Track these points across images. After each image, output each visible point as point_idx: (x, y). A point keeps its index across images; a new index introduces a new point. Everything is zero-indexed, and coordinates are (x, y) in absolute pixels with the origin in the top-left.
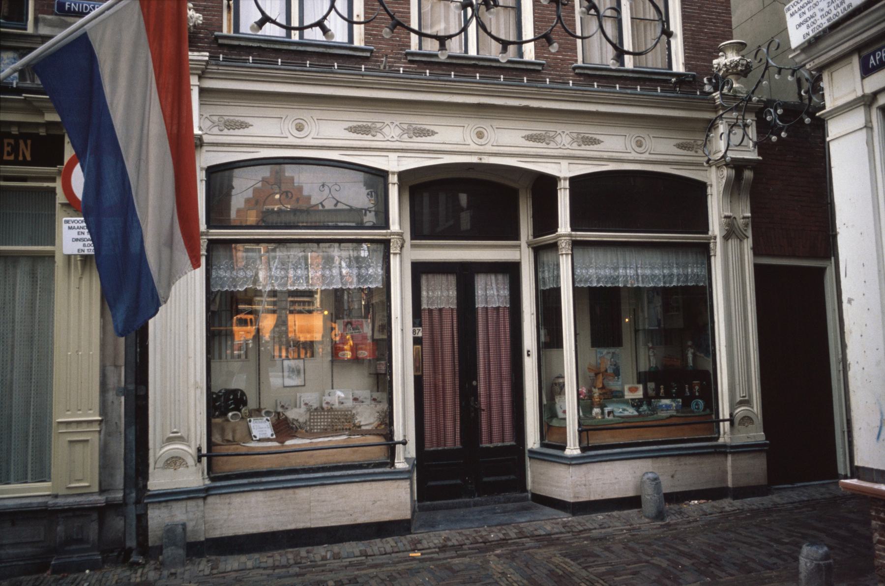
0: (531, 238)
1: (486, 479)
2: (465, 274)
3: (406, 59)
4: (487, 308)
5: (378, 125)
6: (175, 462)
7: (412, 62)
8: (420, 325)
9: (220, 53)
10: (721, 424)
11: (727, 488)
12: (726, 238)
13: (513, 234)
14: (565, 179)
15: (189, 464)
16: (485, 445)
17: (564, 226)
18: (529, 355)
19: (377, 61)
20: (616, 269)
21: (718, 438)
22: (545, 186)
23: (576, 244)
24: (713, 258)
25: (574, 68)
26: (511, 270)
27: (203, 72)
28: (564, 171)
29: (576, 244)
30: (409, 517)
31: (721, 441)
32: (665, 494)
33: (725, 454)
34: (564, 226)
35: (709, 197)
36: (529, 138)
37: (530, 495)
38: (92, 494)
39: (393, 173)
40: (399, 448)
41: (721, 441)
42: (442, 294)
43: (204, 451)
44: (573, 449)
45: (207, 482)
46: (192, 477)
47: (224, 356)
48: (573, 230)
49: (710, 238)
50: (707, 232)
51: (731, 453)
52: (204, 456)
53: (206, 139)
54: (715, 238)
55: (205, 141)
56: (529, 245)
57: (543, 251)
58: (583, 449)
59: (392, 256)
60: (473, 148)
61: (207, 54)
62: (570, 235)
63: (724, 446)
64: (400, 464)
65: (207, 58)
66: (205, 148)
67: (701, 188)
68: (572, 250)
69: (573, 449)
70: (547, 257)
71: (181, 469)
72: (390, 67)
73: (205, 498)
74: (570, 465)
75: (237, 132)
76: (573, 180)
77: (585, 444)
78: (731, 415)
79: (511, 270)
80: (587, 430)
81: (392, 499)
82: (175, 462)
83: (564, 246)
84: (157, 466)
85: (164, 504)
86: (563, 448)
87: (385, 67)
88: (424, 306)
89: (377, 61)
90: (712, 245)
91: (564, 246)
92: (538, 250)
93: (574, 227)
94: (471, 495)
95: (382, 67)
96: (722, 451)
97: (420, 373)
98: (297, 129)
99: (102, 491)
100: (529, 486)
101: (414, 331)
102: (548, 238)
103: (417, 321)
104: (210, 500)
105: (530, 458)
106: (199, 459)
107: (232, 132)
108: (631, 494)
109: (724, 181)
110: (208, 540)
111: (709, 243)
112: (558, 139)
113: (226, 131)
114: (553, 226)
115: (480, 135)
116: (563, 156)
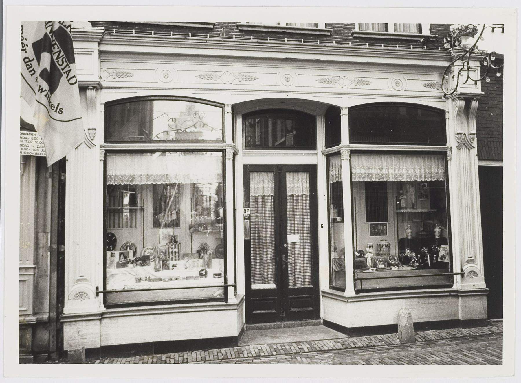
0: (324, 148)
1: (292, 310)
2: (279, 173)
3: (237, 29)
4: (293, 195)
5: (218, 74)
6: (80, 295)
7: (241, 31)
8: (249, 206)
9: (114, 28)
10: (454, 276)
11: (459, 320)
12: (459, 148)
13: (311, 145)
14: (346, 109)
15: (90, 297)
16: (290, 287)
18: (322, 227)
19: (218, 31)
20: (381, 169)
21: (451, 286)
22: (332, 113)
23: (353, 152)
24: (449, 162)
25: (353, 33)
26: (311, 170)
27: (101, 40)
29: (353, 152)
30: (236, 334)
31: (454, 288)
32: (414, 324)
33: (457, 297)
35: (447, 120)
37: (322, 321)
38: (29, 315)
39: (228, 105)
40: (231, 290)
41: (454, 288)
42: (262, 185)
43: (101, 289)
44: (350, 292)
45: (103, 309)
46: (97, 306)
47: (121, 225)
48: (350, 143)
49: (447, 148)
50: (445, 143)
51: (461, 296)
52: (101, 292)
53: (104, 84)
54: (451, 148)
55: (103, 86)
58: (357, 292)
59: (227, 160)
61: (103, 28)
62: (348, 147)
63: (457, 291)
64: (232, 299)
65: (103, 31)
66: (104, 90)
67: (441, 114)
68: (350, 157)
69: (350, 292)
70: (334, 161)
71: (86, 300)
72: (226, 35)
73: (100, 320)
74: (348, 302)
75: (124, 79)
76: (351, 109)
77: (359, 287)
78: (462, 270)
79: (311, 170)
80: (361, 279)
81: (227, 322)
82: (80, 295)
83: (345, 154)
84: (70, 298)
85: (74, 323)
86: (343, 290)
87: (223, 35)
88: (252, 193)
89: (218, 31)
90: (448, 153)
91: (345, 154)
92: (328, 156)
93: (352, 140)
94: (282, 320)
95: (221, 35)
96: (457, 294)
97: (248, 238)
98: (164, 77)
99: (35, 314)
100: (322, 315)
101: (245, 211)
103: (247, 203)
104: (105, 321)
105: (323, 296)
106: (97, 295)
107: (121, 79)
108: (391, 322)
109: (457, 109)
110: (102, 347)
111: (447, 152)
112: (341, 81)
113: (117, 79)
115: (287, 79)
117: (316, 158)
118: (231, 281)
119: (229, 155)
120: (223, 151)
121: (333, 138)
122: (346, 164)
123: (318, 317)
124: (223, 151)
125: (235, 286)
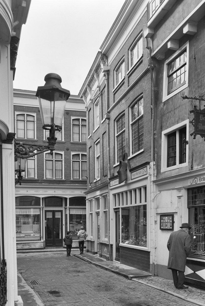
0: (64, 206)
2: (54, 212)
13: (62, 206)
17: (68, 206)
22: (66, 199)
26: (61, 211)
28: (68, 197)
34: (68, 206)
36: (62, 192)
42: (50, 216)
56: (64, 207)
57: (65, 209)
60: (54, 194)
76: (70, 198)
79: (61, 211)
91: (68, 209)
102: (66, 207)
114: (67, 206)
116: (68, 194)
117: (63, 209)
118: (42, 236)
119: (41, 209)
120: (40, 208)
121: (66, 205)
122: (68, 211)
123: (63, 246)
124: (40, 208)
125: (43, 237)
